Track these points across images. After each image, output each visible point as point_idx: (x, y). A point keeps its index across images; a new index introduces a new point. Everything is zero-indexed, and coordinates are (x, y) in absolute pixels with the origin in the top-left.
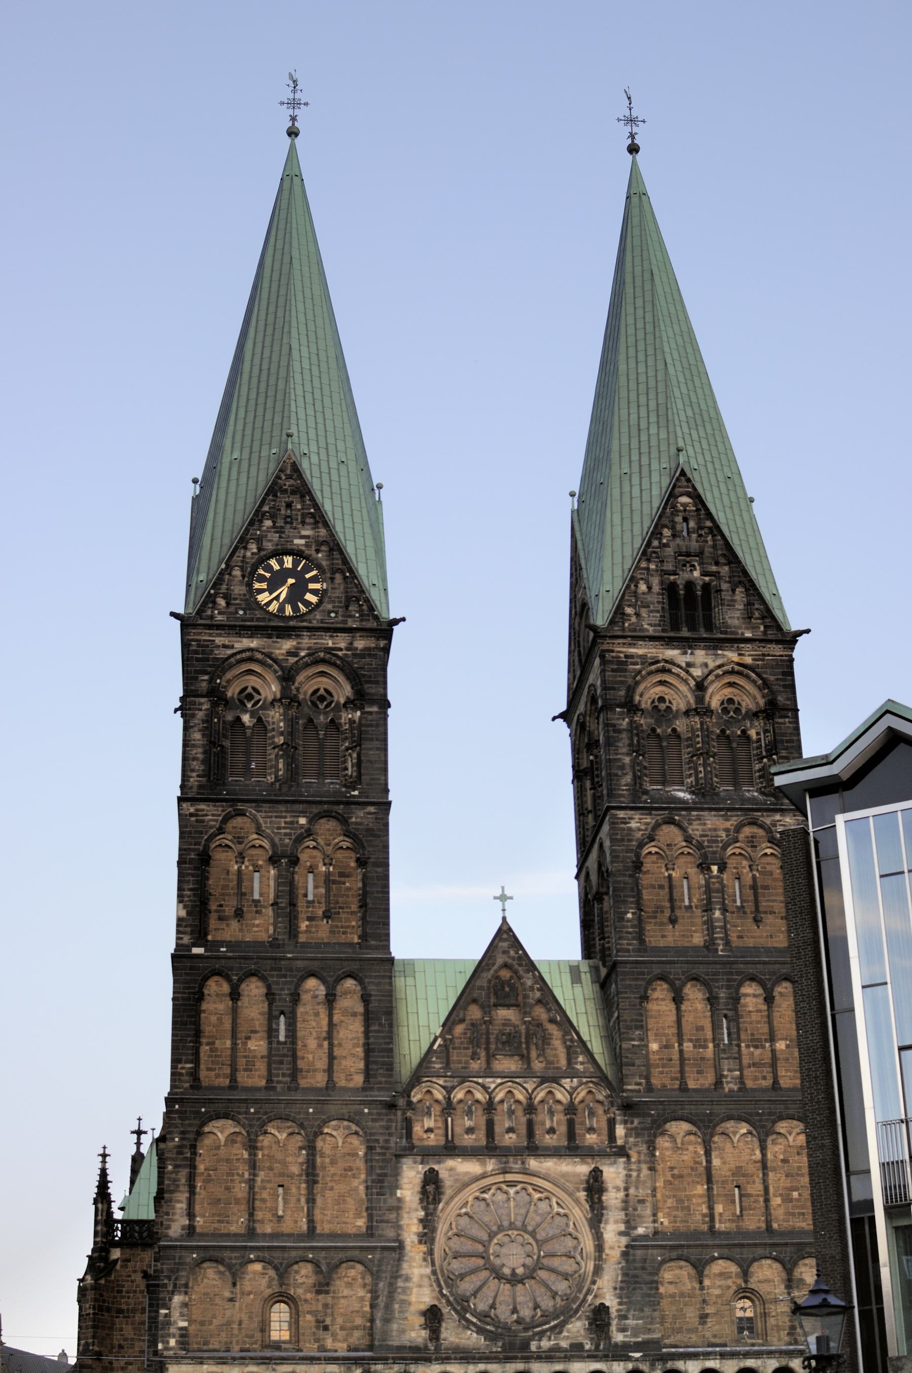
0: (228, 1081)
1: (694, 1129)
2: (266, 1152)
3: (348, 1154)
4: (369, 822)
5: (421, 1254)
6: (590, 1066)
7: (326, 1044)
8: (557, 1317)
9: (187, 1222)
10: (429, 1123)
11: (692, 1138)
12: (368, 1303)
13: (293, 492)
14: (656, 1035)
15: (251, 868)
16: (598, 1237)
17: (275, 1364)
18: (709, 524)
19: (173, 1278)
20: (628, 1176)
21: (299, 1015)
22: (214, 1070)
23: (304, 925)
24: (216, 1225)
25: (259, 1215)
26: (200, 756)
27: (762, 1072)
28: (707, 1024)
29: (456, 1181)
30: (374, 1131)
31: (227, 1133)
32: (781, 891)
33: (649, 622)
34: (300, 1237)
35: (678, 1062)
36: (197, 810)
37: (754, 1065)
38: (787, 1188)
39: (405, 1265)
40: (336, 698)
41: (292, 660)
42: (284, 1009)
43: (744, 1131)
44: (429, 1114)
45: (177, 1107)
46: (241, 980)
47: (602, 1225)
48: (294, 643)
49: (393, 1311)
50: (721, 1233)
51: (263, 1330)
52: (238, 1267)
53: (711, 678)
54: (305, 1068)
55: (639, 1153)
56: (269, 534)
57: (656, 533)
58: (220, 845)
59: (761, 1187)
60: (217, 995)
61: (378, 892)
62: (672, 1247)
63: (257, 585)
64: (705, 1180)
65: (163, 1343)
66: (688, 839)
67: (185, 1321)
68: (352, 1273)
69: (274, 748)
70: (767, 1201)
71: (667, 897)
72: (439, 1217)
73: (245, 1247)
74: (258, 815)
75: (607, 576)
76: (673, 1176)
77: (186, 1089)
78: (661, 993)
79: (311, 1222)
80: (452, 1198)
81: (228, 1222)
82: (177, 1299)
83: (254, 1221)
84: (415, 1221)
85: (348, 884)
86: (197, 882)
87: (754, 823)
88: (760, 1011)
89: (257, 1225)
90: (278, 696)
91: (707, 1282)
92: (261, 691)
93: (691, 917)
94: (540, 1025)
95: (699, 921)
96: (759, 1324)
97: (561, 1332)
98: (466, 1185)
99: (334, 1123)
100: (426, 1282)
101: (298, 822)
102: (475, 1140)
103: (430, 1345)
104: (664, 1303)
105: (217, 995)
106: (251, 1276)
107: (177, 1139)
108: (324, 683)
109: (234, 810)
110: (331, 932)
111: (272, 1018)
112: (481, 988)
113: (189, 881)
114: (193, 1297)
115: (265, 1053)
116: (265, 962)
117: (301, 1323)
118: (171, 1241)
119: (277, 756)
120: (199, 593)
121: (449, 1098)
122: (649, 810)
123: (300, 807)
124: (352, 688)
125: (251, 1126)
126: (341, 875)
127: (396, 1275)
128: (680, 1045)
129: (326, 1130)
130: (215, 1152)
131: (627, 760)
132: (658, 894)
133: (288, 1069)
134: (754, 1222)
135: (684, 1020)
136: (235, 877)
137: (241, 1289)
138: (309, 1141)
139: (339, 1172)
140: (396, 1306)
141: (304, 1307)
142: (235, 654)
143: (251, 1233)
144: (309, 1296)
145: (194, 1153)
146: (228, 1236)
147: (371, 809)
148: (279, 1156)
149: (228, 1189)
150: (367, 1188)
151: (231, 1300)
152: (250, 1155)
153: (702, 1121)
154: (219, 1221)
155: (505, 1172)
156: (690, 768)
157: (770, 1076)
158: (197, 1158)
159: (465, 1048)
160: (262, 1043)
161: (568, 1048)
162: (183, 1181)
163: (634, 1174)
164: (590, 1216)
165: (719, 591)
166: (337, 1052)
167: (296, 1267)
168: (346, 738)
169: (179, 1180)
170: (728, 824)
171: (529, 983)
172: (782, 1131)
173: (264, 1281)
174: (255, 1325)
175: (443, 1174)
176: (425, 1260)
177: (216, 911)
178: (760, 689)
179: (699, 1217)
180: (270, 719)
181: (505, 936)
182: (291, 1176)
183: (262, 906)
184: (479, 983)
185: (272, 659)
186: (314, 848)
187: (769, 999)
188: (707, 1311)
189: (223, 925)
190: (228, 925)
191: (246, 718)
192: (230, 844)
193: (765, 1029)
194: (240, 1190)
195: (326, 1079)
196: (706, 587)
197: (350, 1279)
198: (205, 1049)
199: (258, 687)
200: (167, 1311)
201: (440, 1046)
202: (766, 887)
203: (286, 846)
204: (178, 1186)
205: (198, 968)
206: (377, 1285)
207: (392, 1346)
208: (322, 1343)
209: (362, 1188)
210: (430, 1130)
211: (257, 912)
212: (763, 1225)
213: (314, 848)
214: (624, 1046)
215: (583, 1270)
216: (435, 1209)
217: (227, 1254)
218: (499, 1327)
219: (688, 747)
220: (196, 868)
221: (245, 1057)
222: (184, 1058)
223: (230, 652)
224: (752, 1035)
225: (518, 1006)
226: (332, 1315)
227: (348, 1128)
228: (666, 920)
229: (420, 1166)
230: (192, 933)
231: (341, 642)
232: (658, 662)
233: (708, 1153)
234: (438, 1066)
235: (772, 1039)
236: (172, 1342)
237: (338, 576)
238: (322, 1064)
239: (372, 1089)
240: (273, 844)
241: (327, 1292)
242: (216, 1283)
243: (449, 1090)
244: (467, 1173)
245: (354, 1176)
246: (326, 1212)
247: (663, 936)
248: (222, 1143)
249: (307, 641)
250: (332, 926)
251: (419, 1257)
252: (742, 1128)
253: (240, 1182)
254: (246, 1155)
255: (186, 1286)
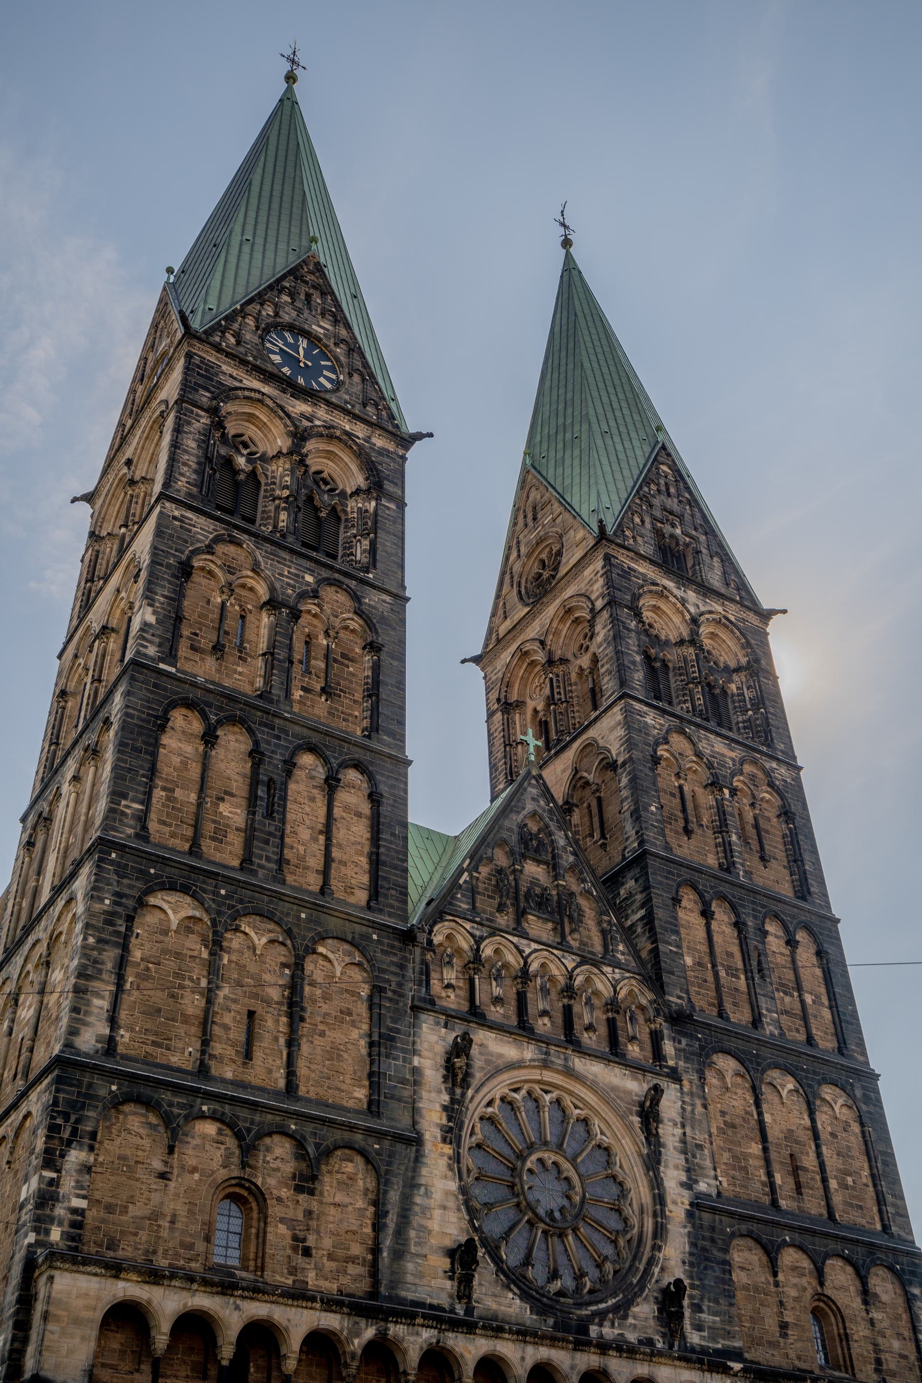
0: (187, 846)
1: (742, 1070)
2: (234, 958)
3: (347, 991)
4: (384, 609)
5: (446, 1158)
6: (631, 958)
7: (322, 838)
8: (614, 1294)
9: (107, 1031)
10: (450, 975)
11: (739, 1080)
12: (369, 1222)
13: (314, 287)
14: (688, 948)
15: (237, 608)
16: (656, 1183)
17: (243, 1298)
18: (687, 495)
19: (73, 1118)
20: (682, 1108)
21: (290, 793)
22: (170, 825)
23: (297, 694)
24: (149, 1049)
25: (217, 1048)
26: (194, 466)
27: (794, 1023)
28: (736, 950)
29: (488, 1062)
30: (384, 967)
31: (183, 914)
32: (780, 840)
33: (647, 549)
34: (276, 1094)
35: (713, 986)
36: (182, 516)
37: (786, 1012)
38: (839, 1170)
39: (424, 1171)
40: (341, 487)
41: (306, 423)
42: (275, 777)
43: (790, 1086)
44: (449, 963)
45: (114, 855)
46: (220, 723)
47: (662, 1169)
48: (309, 409)
49: (407, 1240)
50: (786, 1213)
51: (208, 1239)
52: (182, 1122)
53: (702, 618)
54: (294, 861)
55: (691, 1082)
56: (287, 309)
57: (647, 481)
58: (202, 569)
59: (816, 1163)
60: (184, 732)
61: (392, 685)
62: (743, 1218)
63: (268, 345)
64: (758, 1137)
65: (37, 1230)
66: (699, 755)
67: (84, 1197)
68: (349, 1168)
69: (273, 500)
70: (824, 1180)
71: (680, 807)
72: (467, 1109)
73: (197, 1090)
74: (257, 553)
75: (604, 497)
76: (725, 1123)
77: (129, 836)
78: (689, 899)
79: (291, 1074)
80: (482, 1085)
81: (169, 1049)
82: (76, 1156)
83: (212, 1056)
84: (438, 1107)
85: (351, 669)
86: (174, 591)
87: (754, 762)
88: (782, 954)
89: (212, 1063)
90: (285, 451)
91: (781, 1277)
92: (259, 444)
93: (703, 836)
94: (572, 894)
95: (711, 842)
96: (840, 1351)
97: (625, 1317)
98: (499, 1071)
99: (330, 941)
100: (451, 1204)
101: (303, 578)
102: (504, 1016)
103: (458, 1306)
104: (740, 1295)
105: (184, 732)
106: (197, 1141)
107: (107, 902)
108: (329, 468)
109: (229, 535)
110: (329, 713)
111: (254, 782)
112: (509, 830)
113: (164, 587)
114: (101, 1159)
115: (243, 826)
116: (253, 711)
117: (270, 1237)
118: (79, 1055)
119: (277, 508)
120: (208, 317)
121: (478, 950)
122: (663, 712)
123: (308, 564)
124: (367, 479)
125: (219, 913)
126: (344, 656)
127: (412, 1185)
128: (714, 966)
129: (321, 949)
130: (161, 938)
131: (638, 658)
132: (671, 801)
133: (273, 853)
134: (814, 1206)
135: (715, 939)
136: (217, 611)
137: (180, 1160)
138: (297, 956)
139: (334, 1014)
140: (412, 1234)
141: (274, 1210)
142: (244, 389)
143: (203, 1071)
144: (285, 1193)
145: (129, 929)
146: (169, 1068)
147: (388, 599)
148: (252, 968)
149: (173, 996)
150: (371, 1044)
151: (163, 1176)
152: (211, 954)
153: (751, 1062)
154: (154, 1043)
155: (545, 1065)
156: (684, 695)
157: (803, 1030)
158: (133, 940)
159: (489, 896)
160: (239, 811)
161: (604, 932)
162: (109, 966)
163: (689, 1108)
164: (645, 1151)
165: (698, 552)
166: (336, 853)
167: (267, 1141)
168: (353, 526)
169: (103, 963)
170: (733, 755)
171: (562, 842)
172: (828, 1098)
173: (219, 1153)
174: (195, 1228)
175: (475, 1051)
176: (450, 1168)
177: (190, 638)
178: (743, 647)
179: (758, 1185)
180: (269, 474)
181: (533, 782)
182: (268, 1002)
183: (246, 654)
184: (507, 823)
185: (285, 412)
186: (315, 616)
187: (791, 943)
188: (787, 1319)
189: (197, 657)
190: (202, 659)
191: (241, 461)
192: (217, 570)
193: (790, 975)
194: (193, 1003)
195: (320, 883)
196: (687, 545)
197: (345, 1176)
198: (159, 794)
199: (256, 439)
200: (54, 1175)
201: (465, 882)
202: (767, 832)
203: (290, 597)
204: (100, 971)
205: (165, 689)
206: (386, 1192)
207: (406, 1299)
208: (300, 1277)
209: (363, 1043)
210: (449, 986)
211: (240, 658)
212: (825, 1212)
213: (315, 616)
214: (662, 948)
215: (635, 1231)
216: (463, 1095)
217: (166, 1096)
218: (543, 1295)
219: (681, 675)
220: (173, 576)
221: (214, 822)
222: (131, 794)
223: (237, 384)
224: (780, 978)
225: (546, 863)
226: (318, 1232)
227: (350, 954)
228: (681, 830)
229: (443, 1030)
230: (160, 645)
231: (360, 431)
232: (657, 585)
233: (758, 1104)
234: (465, 906)
235: (799, 988)
236: (55, 1235)
237: (356, 378)
238: (316, 862)
239: (381, 911)
240: (272, 589)
241: (311, 1192)
242: (141, 1142)
243: (479, 941)
244: (501, 1056)
245: (353, 1024)
246: (313, 1067)
247: (680, 846)
248: (174, 927)
249: (322, 414)
250: (331, 707)
251: (443, 1163)
252: (789, 1082)
253: (193, 992)
254: (205, 954)
255: (93, 1135)
